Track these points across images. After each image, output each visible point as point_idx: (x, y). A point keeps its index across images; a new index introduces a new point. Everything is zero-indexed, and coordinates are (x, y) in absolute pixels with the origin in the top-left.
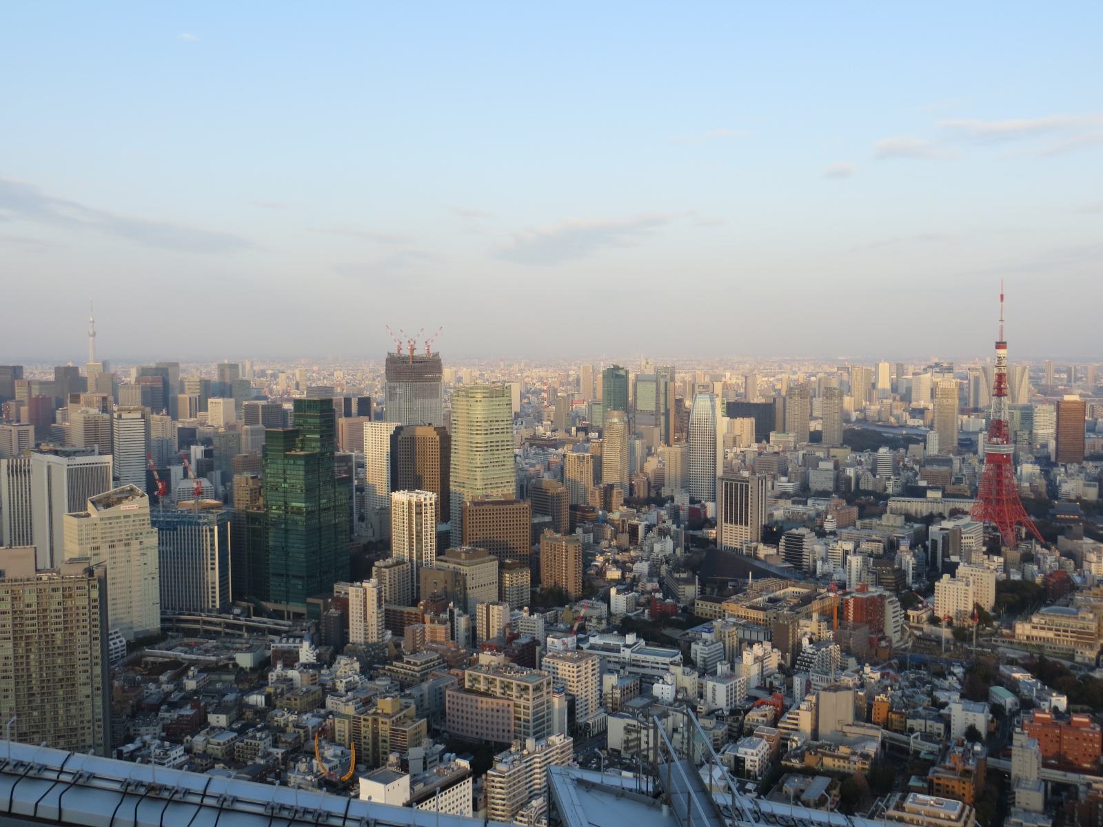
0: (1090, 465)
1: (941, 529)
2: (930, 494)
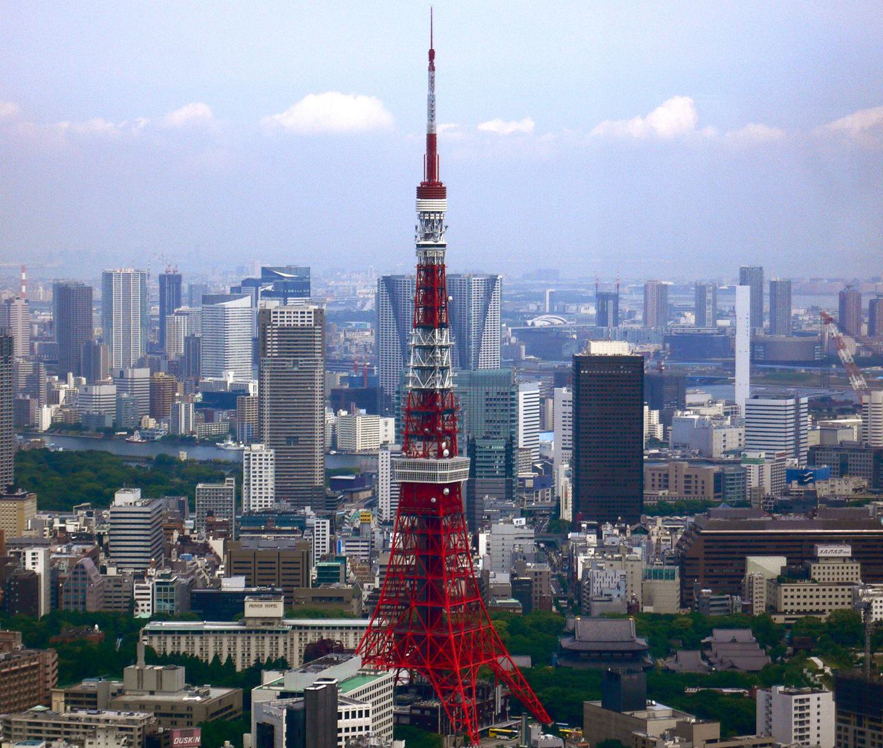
0: (658, 528)
1: (284, 695)
2: (253, 609)
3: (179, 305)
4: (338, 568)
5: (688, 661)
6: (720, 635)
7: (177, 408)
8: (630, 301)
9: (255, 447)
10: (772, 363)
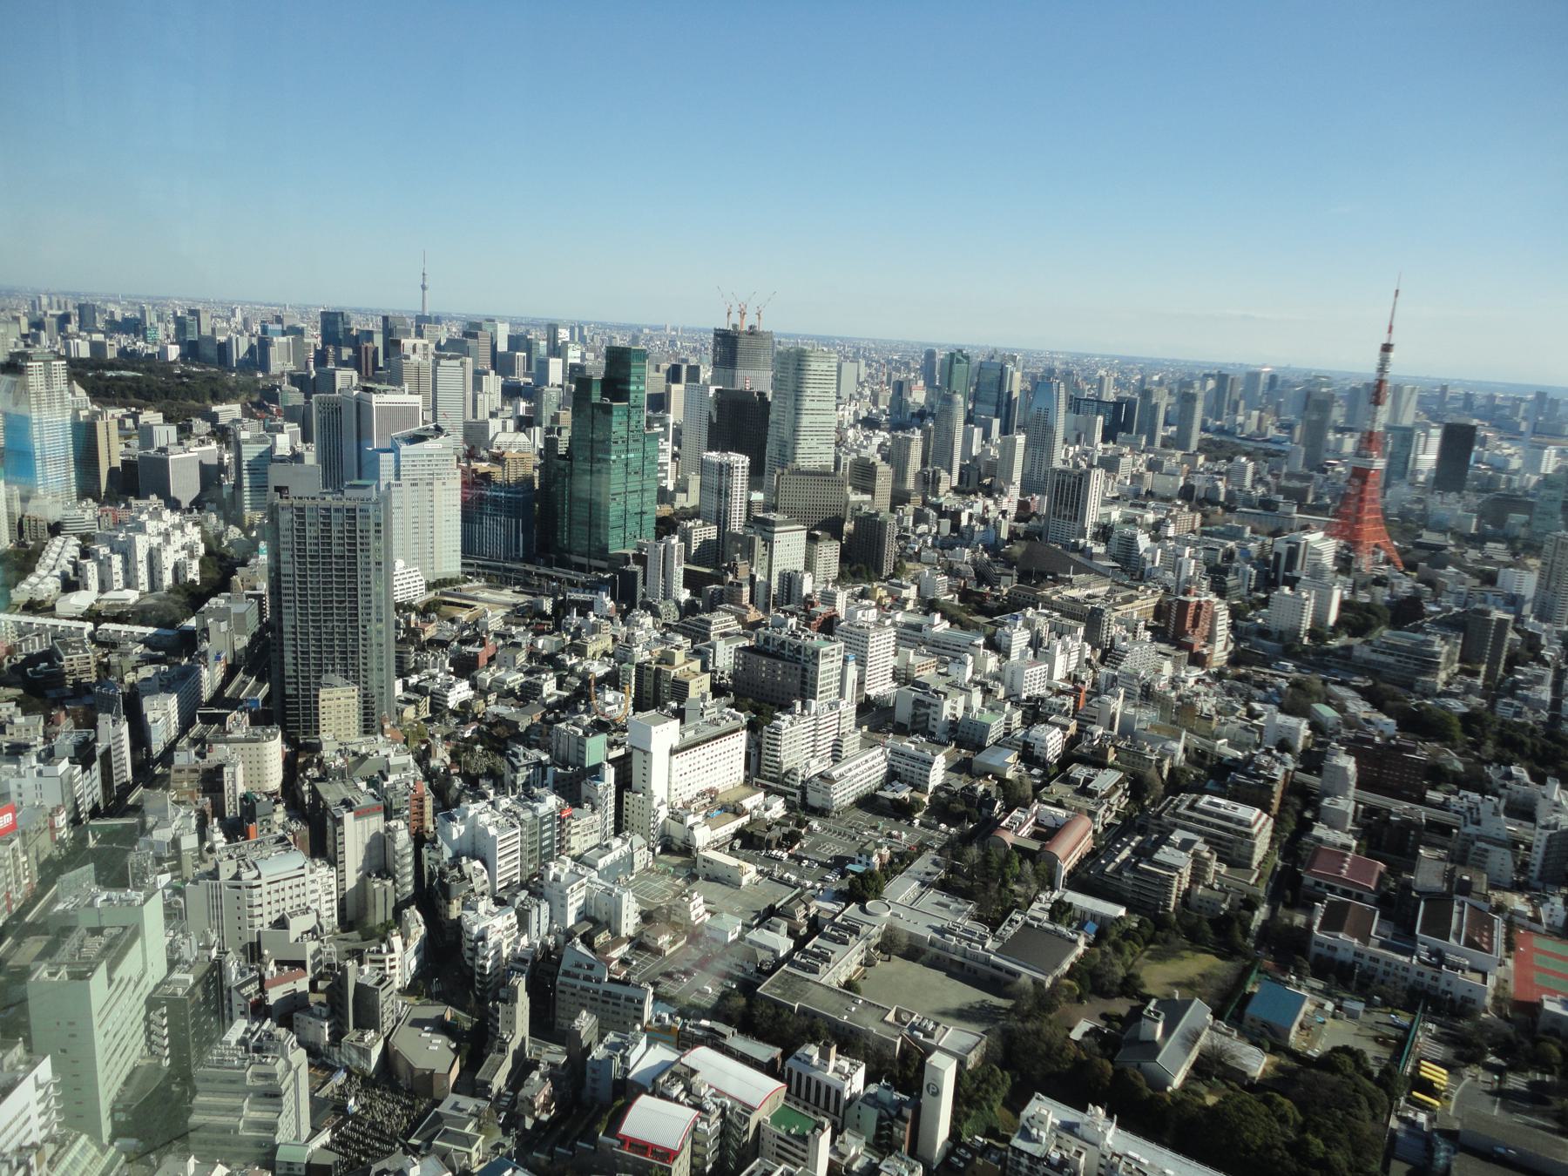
5: (1473, 554)
6: (1490, 545)
8: (1479, 401)
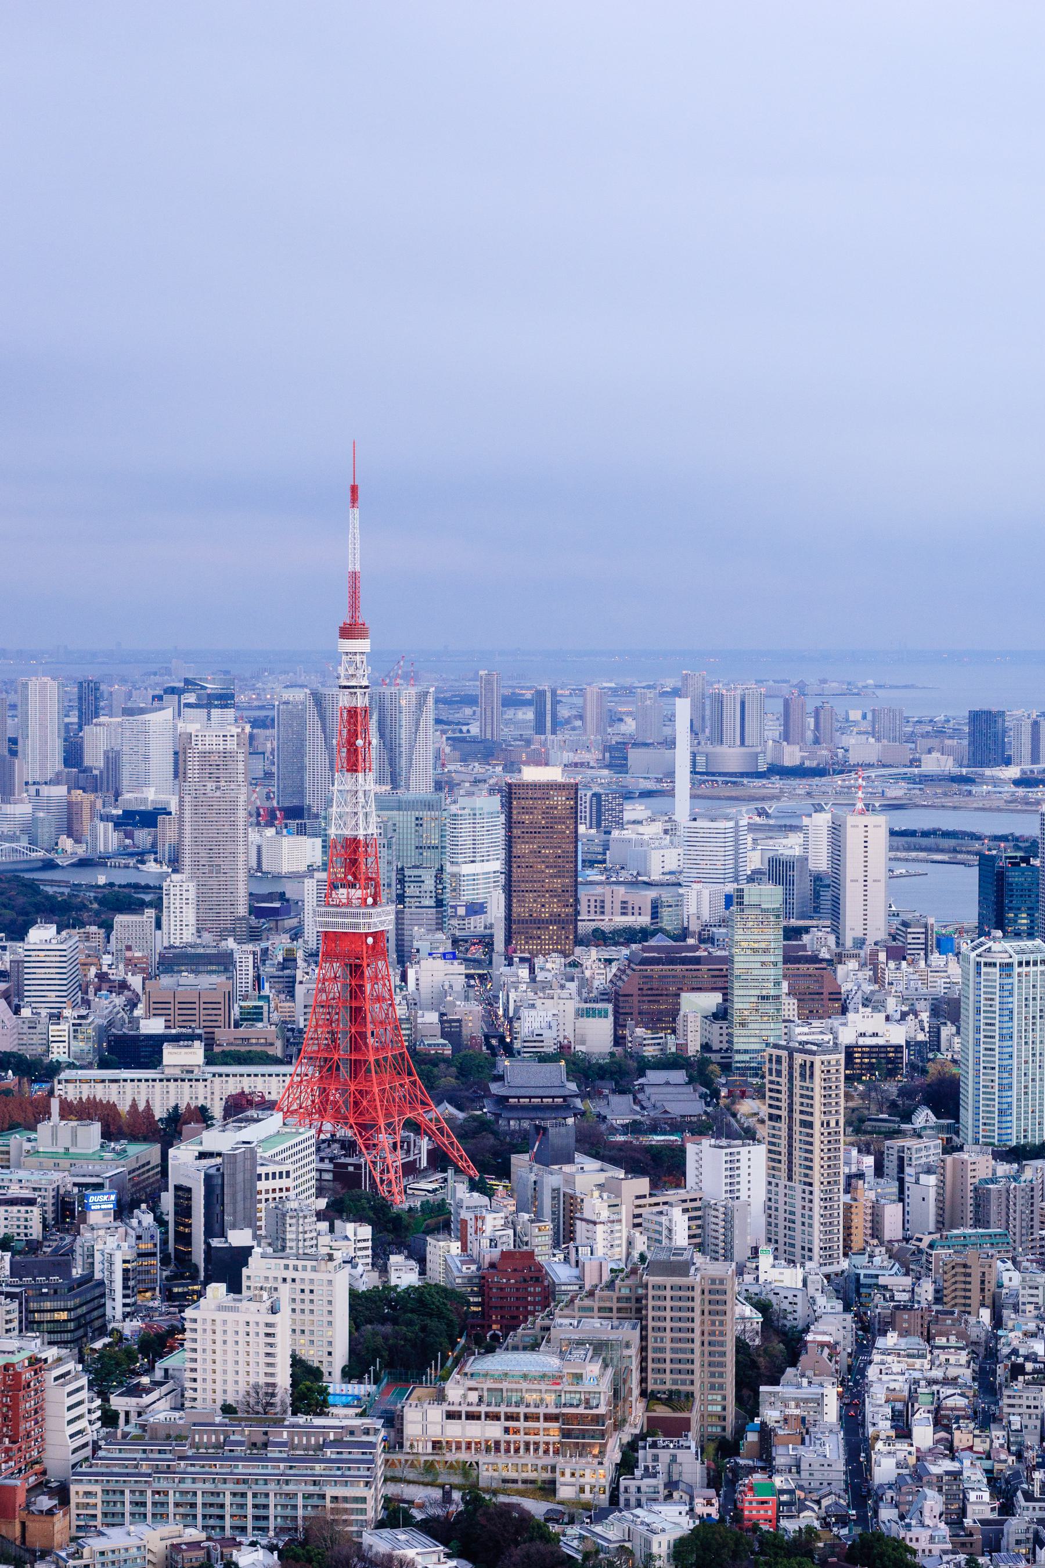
1: (202, 1155)
2: (171, 1055)
3: (97, 716)
4: (261, 1007)
6: (653, 1076)
7: (94, 829)
9: (175, 877)
10: (713, 774)
